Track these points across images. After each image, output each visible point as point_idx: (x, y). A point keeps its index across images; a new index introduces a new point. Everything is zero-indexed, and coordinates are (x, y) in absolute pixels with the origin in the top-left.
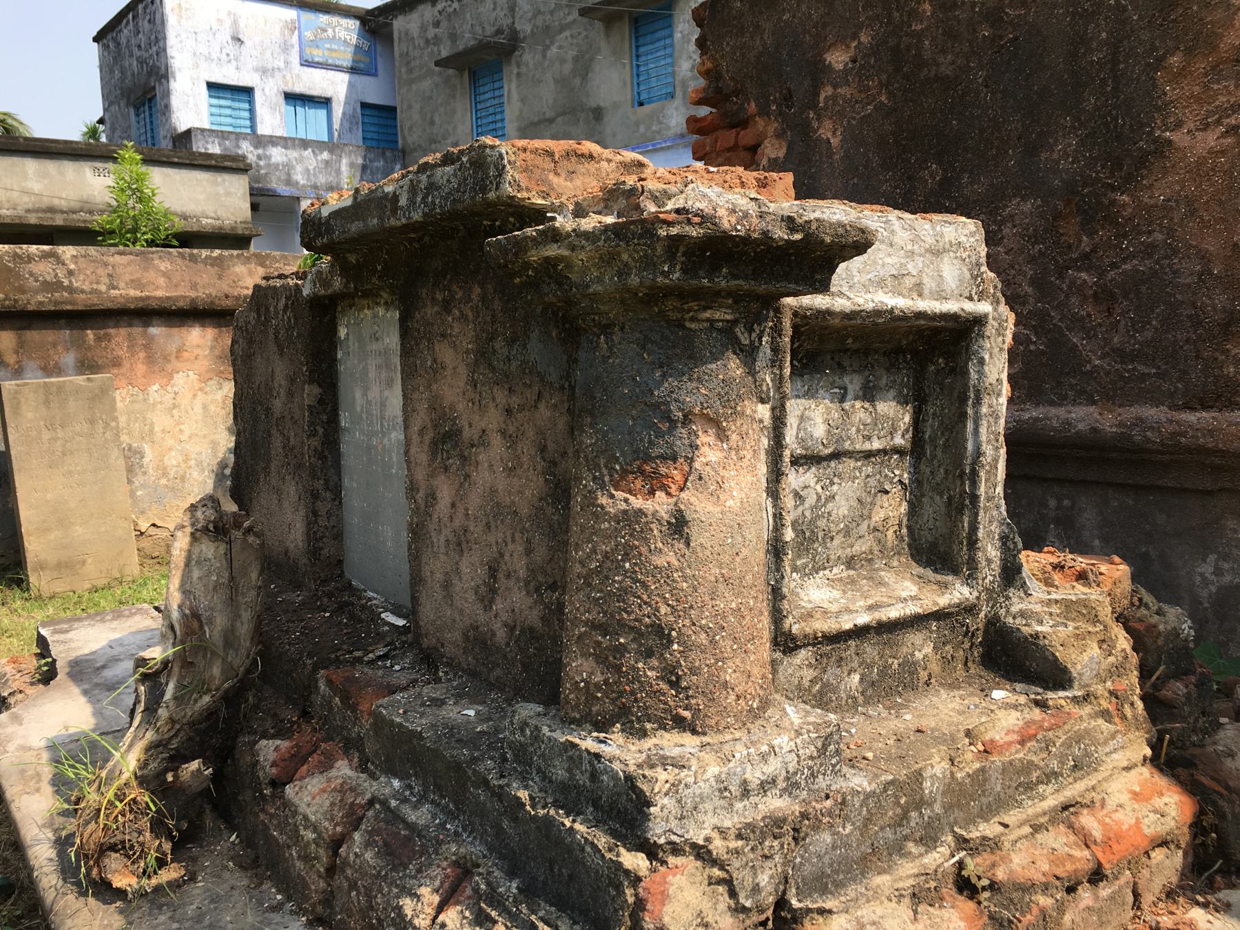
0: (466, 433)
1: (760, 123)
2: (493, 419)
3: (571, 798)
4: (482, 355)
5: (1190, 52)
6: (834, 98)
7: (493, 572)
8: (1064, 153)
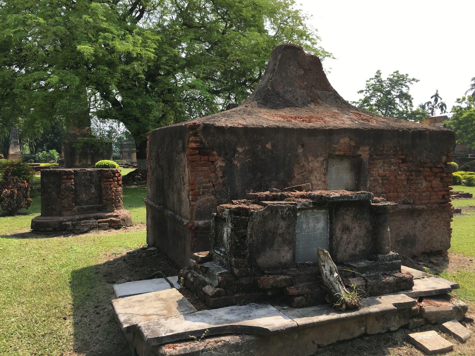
0: (351, 227)
1: (217, 157)
2: (356, 225)
3: (391, 260)
4: (355, 216)
5: (298, 165)
6: (238, 157)
7: (356, 245)
8: (281, 175)
